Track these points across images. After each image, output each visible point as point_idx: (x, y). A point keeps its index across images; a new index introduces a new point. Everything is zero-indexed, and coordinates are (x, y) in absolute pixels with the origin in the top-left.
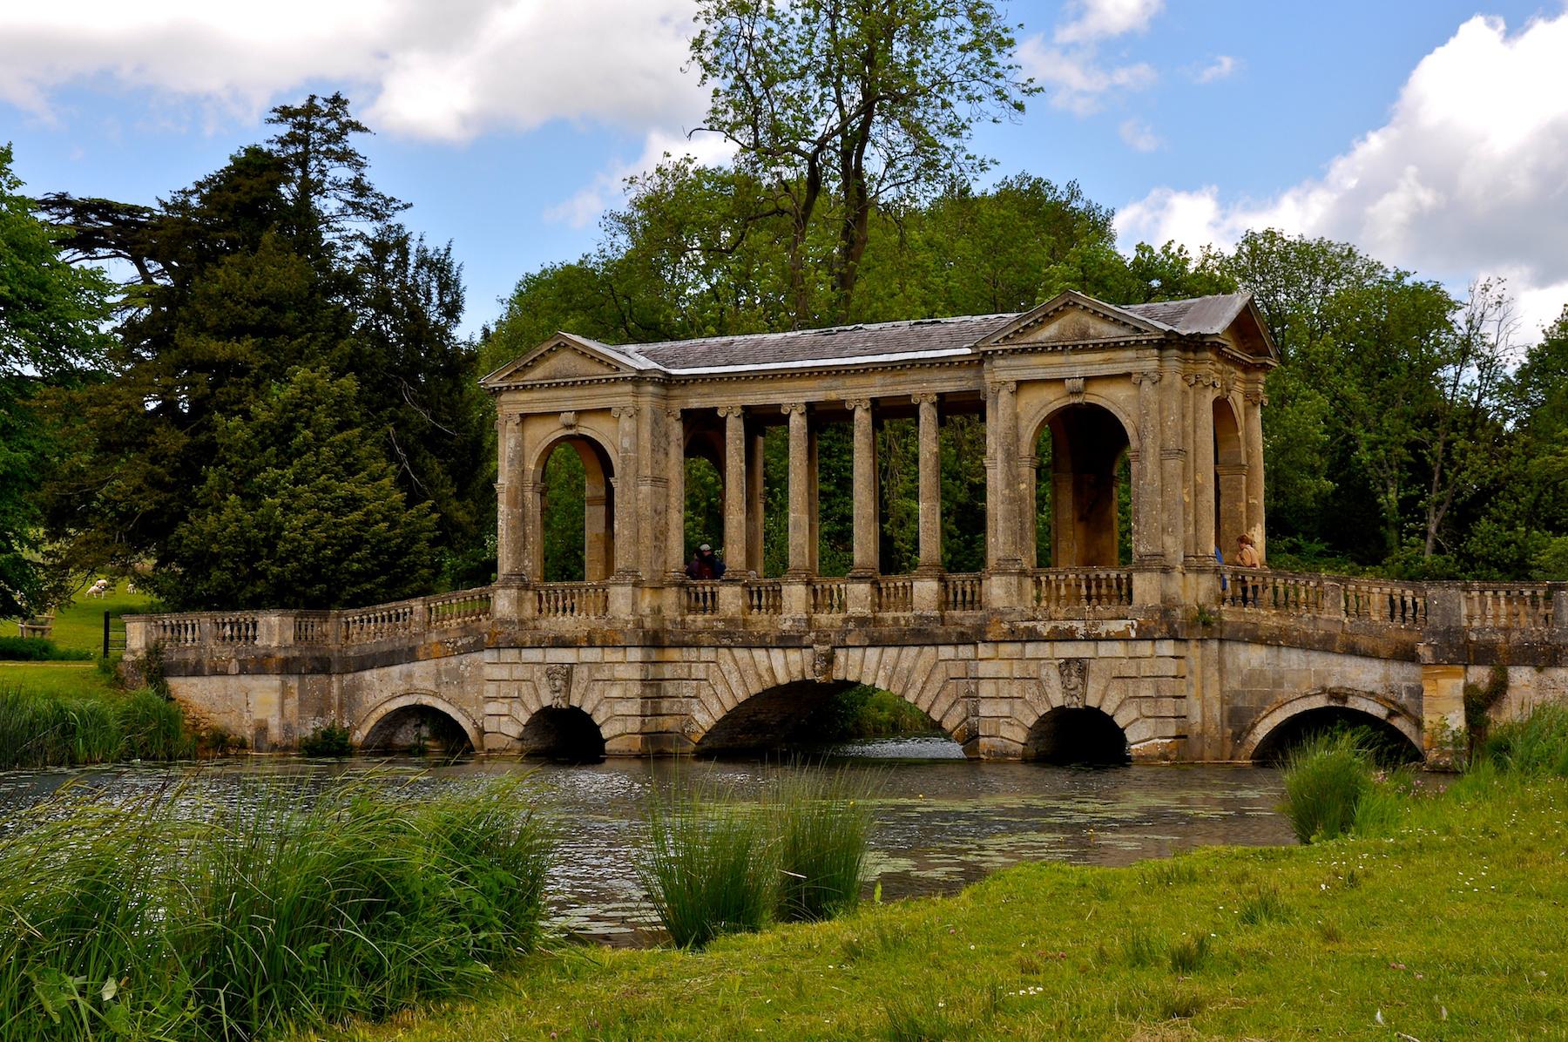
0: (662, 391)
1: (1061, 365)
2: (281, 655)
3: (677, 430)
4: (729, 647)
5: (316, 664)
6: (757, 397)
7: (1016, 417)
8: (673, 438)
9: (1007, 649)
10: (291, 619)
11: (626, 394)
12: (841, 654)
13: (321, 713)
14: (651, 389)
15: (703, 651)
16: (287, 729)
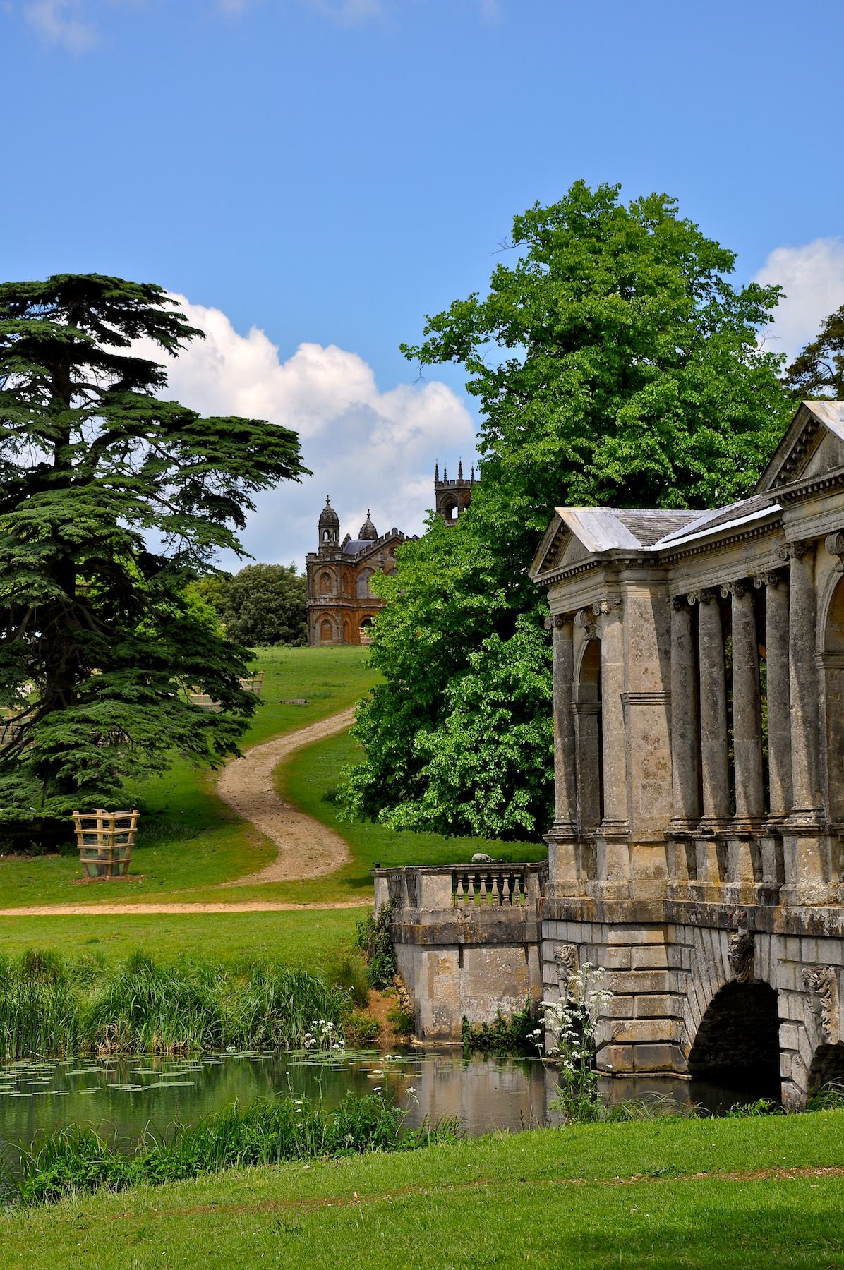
0: (660, 575)
1: (819, 515)
2: (427, 921)
3: (679, 622)
4: (700, 928)
5: (496, 931)
6: (709, 581)
7: (812, 595)
8: (674, 636)
9: (793, 945)
10: (448, 878)
11: (597, 586)
12: (757, 938)
13: (512, 991)
14: (626, 574)
15: (688, 930)
16: (441, 1012)
